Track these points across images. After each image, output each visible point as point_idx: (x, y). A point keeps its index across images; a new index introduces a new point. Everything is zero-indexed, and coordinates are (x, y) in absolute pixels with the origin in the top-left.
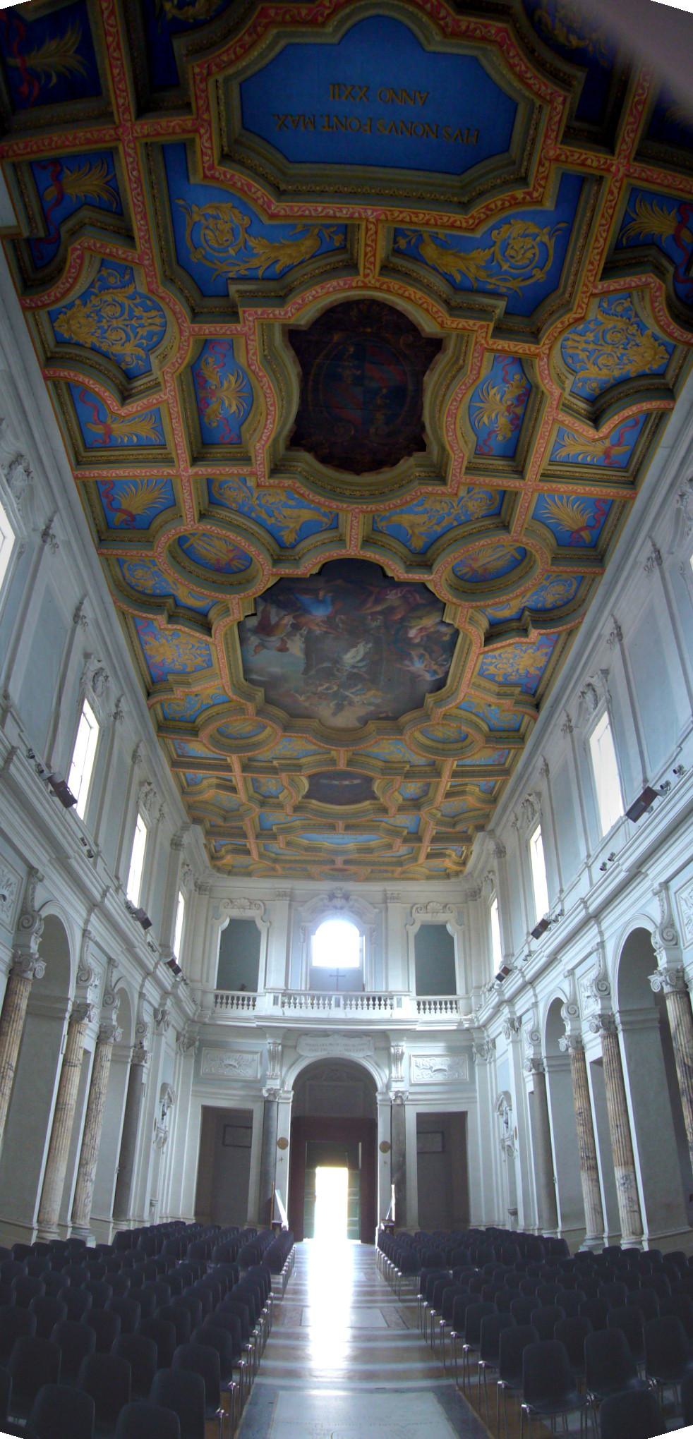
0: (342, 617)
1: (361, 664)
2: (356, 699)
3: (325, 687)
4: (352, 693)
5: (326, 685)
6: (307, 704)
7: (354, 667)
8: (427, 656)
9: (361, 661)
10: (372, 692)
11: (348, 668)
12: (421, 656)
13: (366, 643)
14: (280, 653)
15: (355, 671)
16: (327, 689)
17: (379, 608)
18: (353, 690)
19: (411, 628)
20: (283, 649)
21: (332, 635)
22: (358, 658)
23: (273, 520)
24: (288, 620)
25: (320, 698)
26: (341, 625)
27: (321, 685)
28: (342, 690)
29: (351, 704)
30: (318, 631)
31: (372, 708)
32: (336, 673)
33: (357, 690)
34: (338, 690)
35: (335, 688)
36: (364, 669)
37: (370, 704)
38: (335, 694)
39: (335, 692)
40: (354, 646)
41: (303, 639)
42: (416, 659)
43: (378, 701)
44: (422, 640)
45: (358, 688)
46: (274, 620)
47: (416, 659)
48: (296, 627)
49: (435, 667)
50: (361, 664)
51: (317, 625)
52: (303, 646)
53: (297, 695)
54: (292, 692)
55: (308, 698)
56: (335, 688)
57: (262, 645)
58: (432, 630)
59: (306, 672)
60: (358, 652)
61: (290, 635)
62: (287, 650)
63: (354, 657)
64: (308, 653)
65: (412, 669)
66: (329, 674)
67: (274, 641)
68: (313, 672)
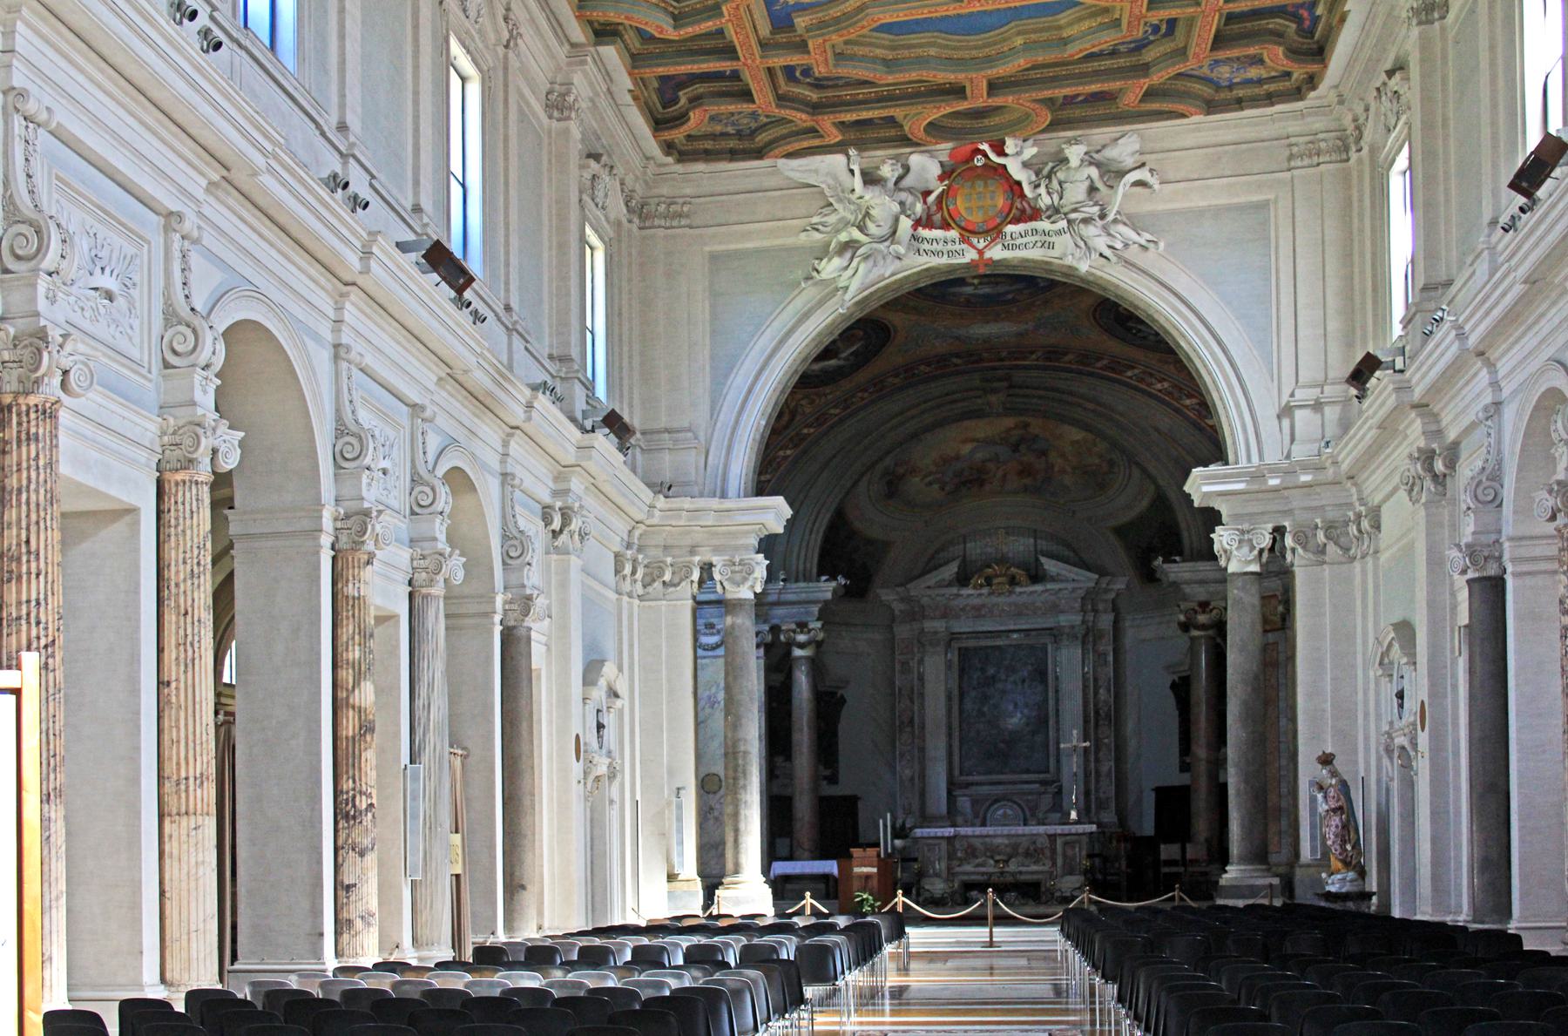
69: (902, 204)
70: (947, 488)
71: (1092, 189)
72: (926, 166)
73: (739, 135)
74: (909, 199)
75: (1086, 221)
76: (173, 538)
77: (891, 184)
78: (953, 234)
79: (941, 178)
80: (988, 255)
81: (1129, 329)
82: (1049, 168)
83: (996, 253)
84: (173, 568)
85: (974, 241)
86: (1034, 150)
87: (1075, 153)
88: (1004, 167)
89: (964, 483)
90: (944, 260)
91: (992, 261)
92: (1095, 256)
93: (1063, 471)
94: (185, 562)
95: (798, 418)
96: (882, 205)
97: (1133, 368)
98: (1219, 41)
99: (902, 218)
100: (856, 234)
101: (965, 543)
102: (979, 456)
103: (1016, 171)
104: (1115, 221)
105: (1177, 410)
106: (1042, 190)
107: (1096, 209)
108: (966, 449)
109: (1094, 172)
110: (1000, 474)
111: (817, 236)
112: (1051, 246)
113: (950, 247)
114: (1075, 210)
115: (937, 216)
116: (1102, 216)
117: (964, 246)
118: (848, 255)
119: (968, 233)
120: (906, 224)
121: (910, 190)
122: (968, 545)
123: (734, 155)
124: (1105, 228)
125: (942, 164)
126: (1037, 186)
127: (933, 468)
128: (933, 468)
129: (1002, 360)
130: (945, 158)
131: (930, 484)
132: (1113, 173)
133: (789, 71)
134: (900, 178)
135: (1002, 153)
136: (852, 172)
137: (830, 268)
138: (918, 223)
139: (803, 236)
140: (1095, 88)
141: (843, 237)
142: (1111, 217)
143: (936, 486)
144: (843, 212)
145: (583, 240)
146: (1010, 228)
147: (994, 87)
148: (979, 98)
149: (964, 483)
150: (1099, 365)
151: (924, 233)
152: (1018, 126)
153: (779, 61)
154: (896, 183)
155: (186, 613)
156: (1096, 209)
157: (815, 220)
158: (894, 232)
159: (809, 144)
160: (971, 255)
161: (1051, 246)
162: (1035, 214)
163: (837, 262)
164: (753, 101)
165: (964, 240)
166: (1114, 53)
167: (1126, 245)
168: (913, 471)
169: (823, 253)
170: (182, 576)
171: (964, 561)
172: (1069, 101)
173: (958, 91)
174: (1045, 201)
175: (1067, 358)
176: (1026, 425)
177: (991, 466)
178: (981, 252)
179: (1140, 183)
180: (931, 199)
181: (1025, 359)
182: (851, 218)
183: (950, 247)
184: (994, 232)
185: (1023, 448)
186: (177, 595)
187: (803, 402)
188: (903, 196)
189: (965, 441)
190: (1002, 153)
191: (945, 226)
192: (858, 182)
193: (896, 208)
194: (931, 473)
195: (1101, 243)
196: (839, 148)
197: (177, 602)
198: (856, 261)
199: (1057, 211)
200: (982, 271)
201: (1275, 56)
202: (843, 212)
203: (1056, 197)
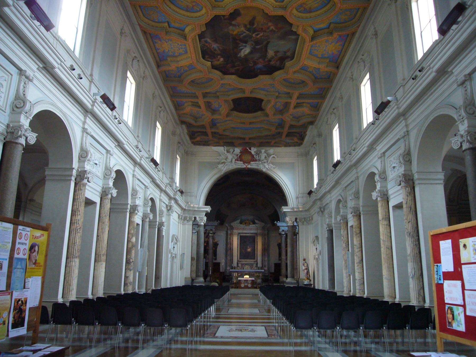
0: (251, 65)
1: (242, 47)
2: (243, 29)
3: (259, 36)
4: (245, 33)
5: (258, 37)
6: (270, 24)
7: (245, 46)
8: (212, 50)
9: (242, 49)
10: (235, 33)
11: (248, 45)
12: (215, 50)
13: (240, 56)
14: (278, 50)
15: (244, 44)
16: (257, 35)
17: (237, 68)
18: (244, 34)
19: (222, 61)
20: (276, 52)
21: (255, 59)
22: (243, 51)
23: (273, 86)
24: (272, 63)
25: (262, 29)
26: (252, 62)
27: (261, 36)
28: (251, 34)
29: (245, 26)
30: (261, 60)
31: (233, 23)
32: (254, 44)
33: (242, 34)
34: (252, 34)
35: (254, 35)
36: (240, 45)
37: (234, 25)
38: (255, 31)
39: (254, 33)
40: (246, 55)
41: (267, 57)
42: (217, 49)
43: (231, 27)
44: (217, 56)
45: (242, 36)
46: (278, 63)
47: (217, 49)
48: (270, 61)
49: (207, 45)
50: (242, 47)
51: (261, 62)
52: (267, 54)
53: (274, 29)
54: (277, 31)
55: (268, 28)
56: (254, 35)
57: (285, 52)
58: (214, 60)
59: (268, 43)
60: (244, 53)
61: (273, 58)
62: (275, 52)
63: (246, 50)
64: (266, 51)
65: (218, 45)
66: (257, 42)
67: (280, 55)
68: (265, 43)
69: (233, 156)
71: (266, 157)
72: (238, 150)
73: (205, 142)
74: (234, 156)
75: (265, 163)
76: (102, 209)
77: (231, 153)
78: (242, 162)
79: (240, 153)
80: (248, 167)
82: (258, 153)
83: (249, 166)
84: (102, 214)
85: (245, 164)
86: (256, 150)
87: (263, 151)
88: (251, 152)
90: (240, 167)
91: (248, 168)
92: (266, 169)
94: (104, 213)
96: (230, 156)
98: (287, 136)
99: (233, 159)
100: (225, 161)
103: (253, 153)
104: (269, 163)
106: (257, 156)
107: (266, 161)
109: (266, 154)
111: (218, 160)
112: (259, 166)
113: (241, 165)
114: (263, 161)
115: (240, 158)
116: (267, 162)
117: (243, 165)
118: (223, 164)
119: (244, 162)
120: (234, 160)
121: (235, 154)
123: (204, 145)
124: (267, 164)
125: (240, 150)
126: (256, 156)
130: (241, 149)
132: (269, 155)
133: (215, 133)
134: (233, 152)
135: (251, 150)
136: (225, 150)
137: (220, 166)
138: (236, 160)
139: (216, 160)
140: (267, 141)
141: (223, 161)
142: (269, 162)
144: (223, 157)
145: (176, 158)
146: (252, 162)
147: (250, 139)
148: (247, 140)
151: (236, 161)
152: (254, 146)
153: (213, 130)
154: (232, 153)
155: (104, 223)
156: (266, 161)
157: (218, 157)
158: (232, 161)
159: (217, 144)
160: (244, 166)
161: (259, 166)
162: (256, 161)
163: (221, 165)
164: (208, 136)
165: (244, 164)
166: (270, 136)
167: (271, 167)
169: (219, 163)
170: (103, 216)
171: (241, 219)
172: (262, 142)
173: (244, 139)
174: (257, 158)
178: (246, 166)
179: (273, 157)
180: (238, 156)
182: (224, 158)
183: (241, 165)
184: (249, 163)
186: (102, 219)
188: (233, 155)
190: (251, 150)
191: (241, 161)
192: (226, 152)
193: (232, 157)
195: (267, 166)
196: (223, 146)
197: (102, 221)
198: (224, 166)
199: (260, 160)
200: (246, 169)
201: (296, 139)
202: (223, 157)
203: (259, 158)
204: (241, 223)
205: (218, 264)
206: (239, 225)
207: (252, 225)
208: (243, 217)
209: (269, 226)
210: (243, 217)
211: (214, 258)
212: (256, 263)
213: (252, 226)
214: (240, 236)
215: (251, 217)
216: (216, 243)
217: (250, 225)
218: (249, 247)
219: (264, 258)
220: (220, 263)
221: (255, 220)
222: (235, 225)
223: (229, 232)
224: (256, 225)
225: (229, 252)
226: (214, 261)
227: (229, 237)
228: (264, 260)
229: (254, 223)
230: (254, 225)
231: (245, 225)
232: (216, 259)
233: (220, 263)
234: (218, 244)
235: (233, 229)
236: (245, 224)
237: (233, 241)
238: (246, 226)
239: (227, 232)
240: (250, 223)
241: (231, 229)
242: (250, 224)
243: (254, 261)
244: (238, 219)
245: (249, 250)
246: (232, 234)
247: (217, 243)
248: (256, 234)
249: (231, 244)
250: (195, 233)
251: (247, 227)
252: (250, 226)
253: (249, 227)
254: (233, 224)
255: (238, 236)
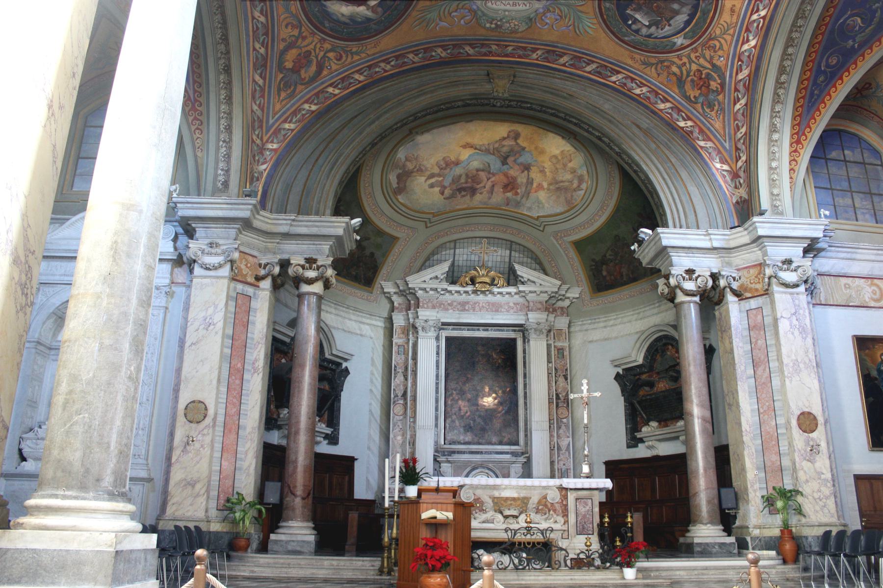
70: (447, 192)
81: (625, 18)
89: (460, 190)
93: (540, 187)
95: (325, 72)
97: (618, 72)
101: (455, 248)
102: (475, 164)
105: (653, 112)
108: (465, 154)
110: (489, 184)
122: (457, 251)
127: (436, 170)
128: (436, 170)
129: (507, 56)
131: (432, 186)
143: (437, 189)
149: (460, 190)
150: (588, 69)
168: (420, 170)
171: (453, 265)
175: (563, 60)
176: (517, 136)
177: (483, 175)
181: (526, 56)
185: (510, 160)
187: (331, 55)
189: (467, 146)
194: (432, 176)
204: (453, 278)
205: (347, 464)
206: (445, 285)
207: (505, 290)
208: (464, 255)
209: (574, 293)
210: (464, 255)
211: (329, 431)
212: (522, 459)
213: (505, 294)
214: (449, 340)
215: (497, 256)
216: (340, 364)
217: (496, 290)
218: (487, 389)
219: (558, 436)
220: (351, 460)
221: (517, 267)
222: (424, 286)
223: (399, 320)
224: (522, 288)
225: (397, 409)
226: (324, 448)
227: (397, 340)
228: (559, 448)
229: (512, 278)
230: (512, 289)
231: (470, 288)
232: (333, 439)
233: (351, 460)
234: (346, 372)
235: (418, 306)
236: (473, 281)
237: (415, 358)
238: (475, 292)
239: (390, 320)
240: (493, 280)
241: (408, 308)
242: (492, 283)
243: (514, 454)
244: (440, 262)
245: (489, 401)
246: (412, 328)
247: (344, 365)
248: (521, 328)
249: (411, 370)
250: (220, 266)
251: (481, 297)
252: (492, 293)
253: (490, 298)
254: (415, 281)
255: (437, 338)
